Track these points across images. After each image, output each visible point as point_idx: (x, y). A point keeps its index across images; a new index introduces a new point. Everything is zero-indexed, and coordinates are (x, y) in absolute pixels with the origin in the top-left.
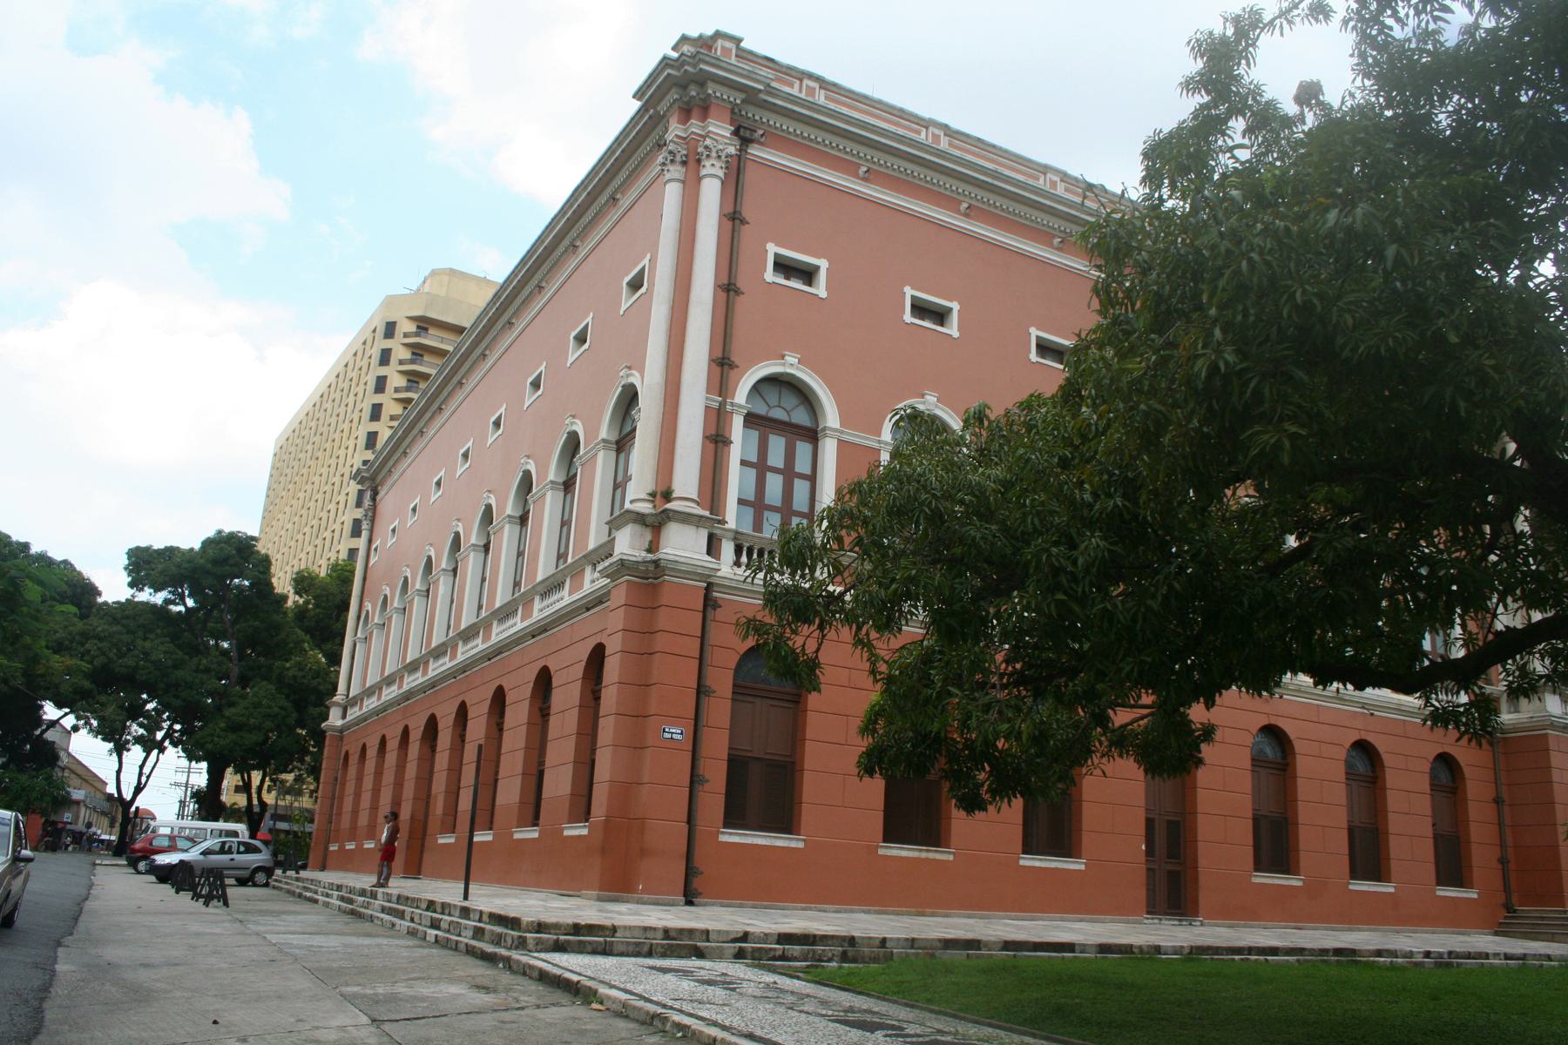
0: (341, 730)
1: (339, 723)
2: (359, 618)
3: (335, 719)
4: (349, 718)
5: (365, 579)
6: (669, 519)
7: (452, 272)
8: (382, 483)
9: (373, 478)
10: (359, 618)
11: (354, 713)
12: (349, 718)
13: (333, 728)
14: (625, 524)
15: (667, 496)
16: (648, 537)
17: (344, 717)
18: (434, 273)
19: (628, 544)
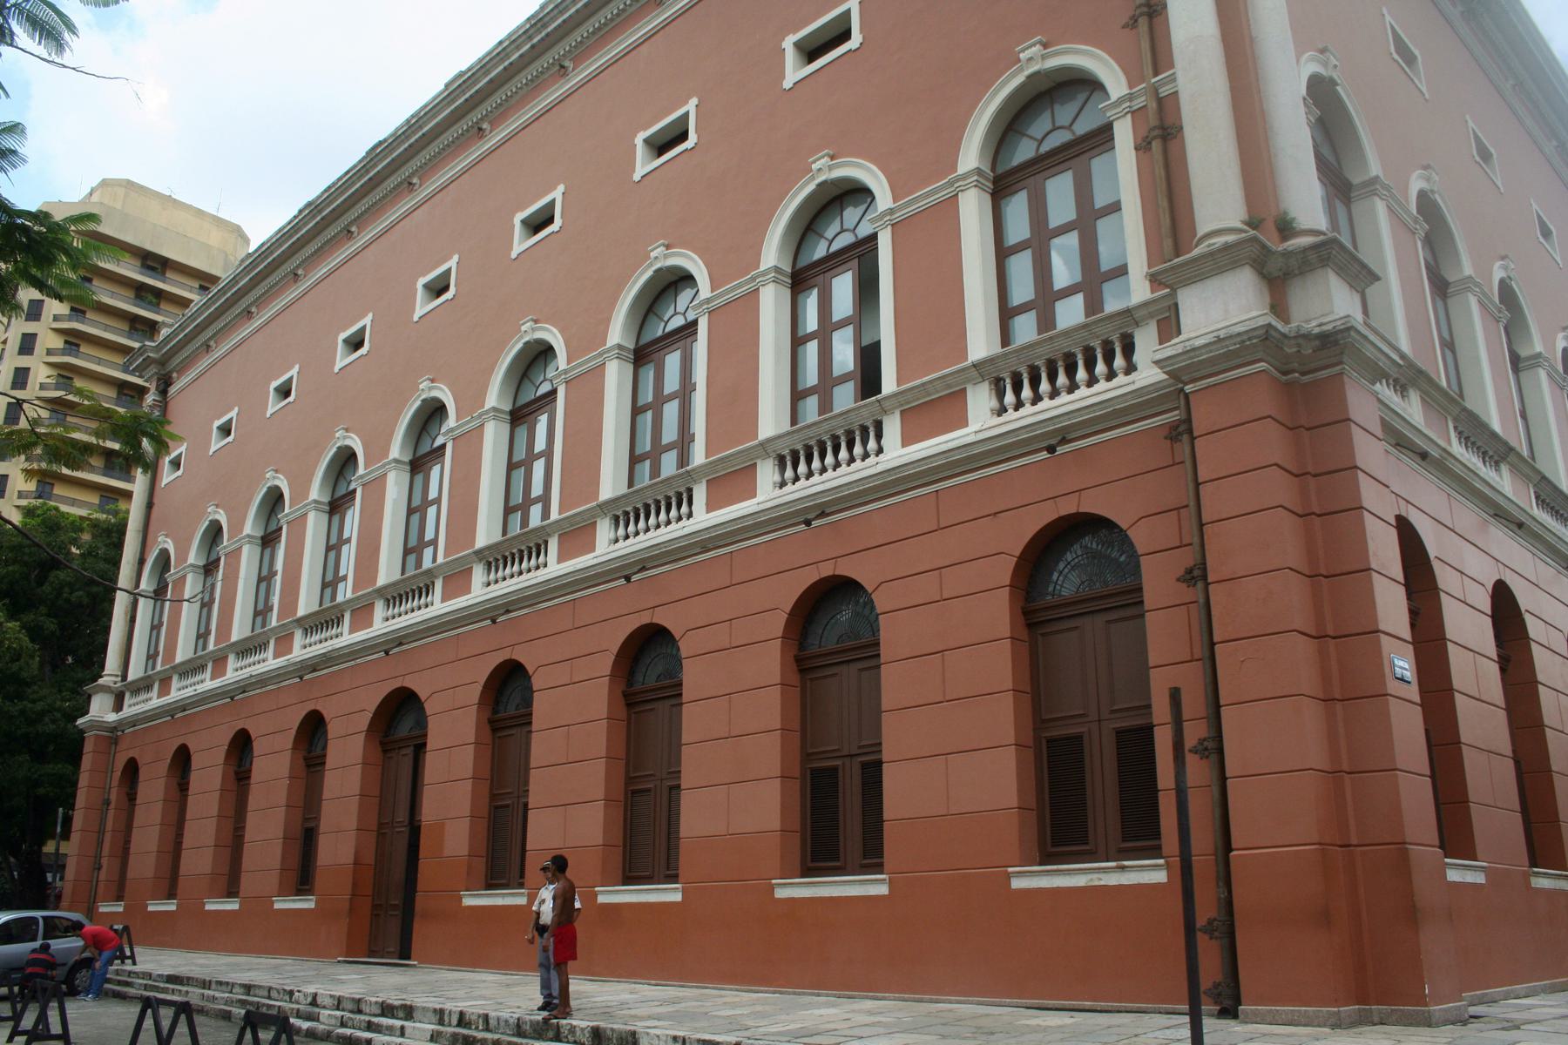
0: (115, 728)
1: (112, 717)
2: (141, 562)
3: (100, 710)
4: (128, 710)
5: (150, 505)
6: (1325, 262)
7: (129, 185)
8: (183, 368)
9: (162, 362)
10: (141, 562)
11: (134, 707)
12: (128, 710)
13: (98, 725)
14: (1234, 265)
15: (1286, 228)
16: (1268, 300)
17: (118, 707)
18: (105, 183)
19: (1221, 309)
